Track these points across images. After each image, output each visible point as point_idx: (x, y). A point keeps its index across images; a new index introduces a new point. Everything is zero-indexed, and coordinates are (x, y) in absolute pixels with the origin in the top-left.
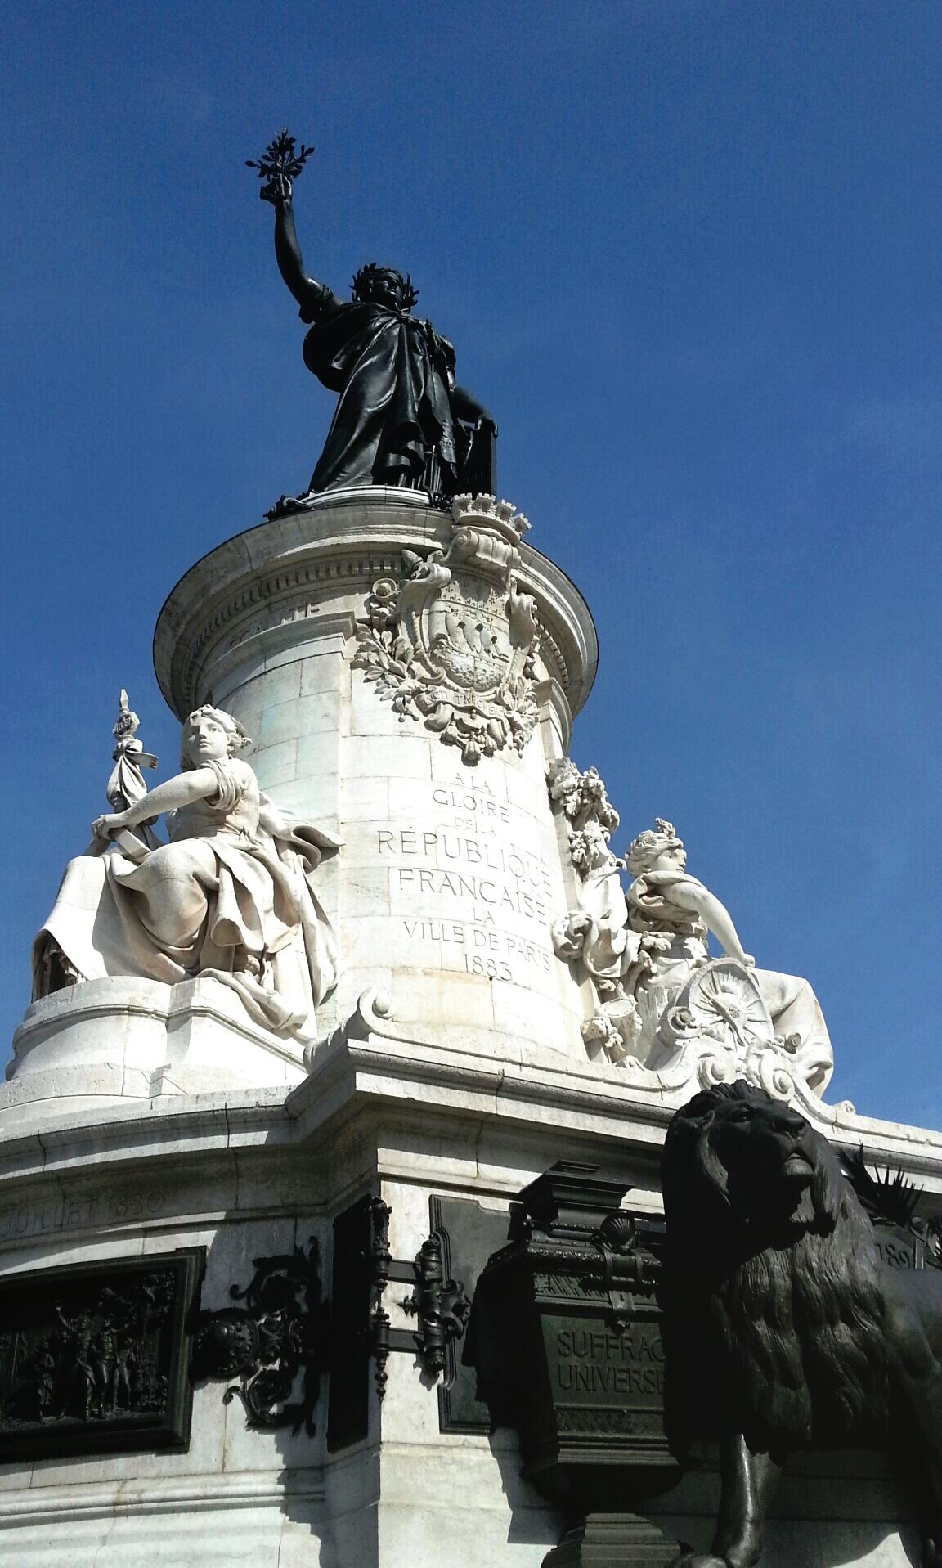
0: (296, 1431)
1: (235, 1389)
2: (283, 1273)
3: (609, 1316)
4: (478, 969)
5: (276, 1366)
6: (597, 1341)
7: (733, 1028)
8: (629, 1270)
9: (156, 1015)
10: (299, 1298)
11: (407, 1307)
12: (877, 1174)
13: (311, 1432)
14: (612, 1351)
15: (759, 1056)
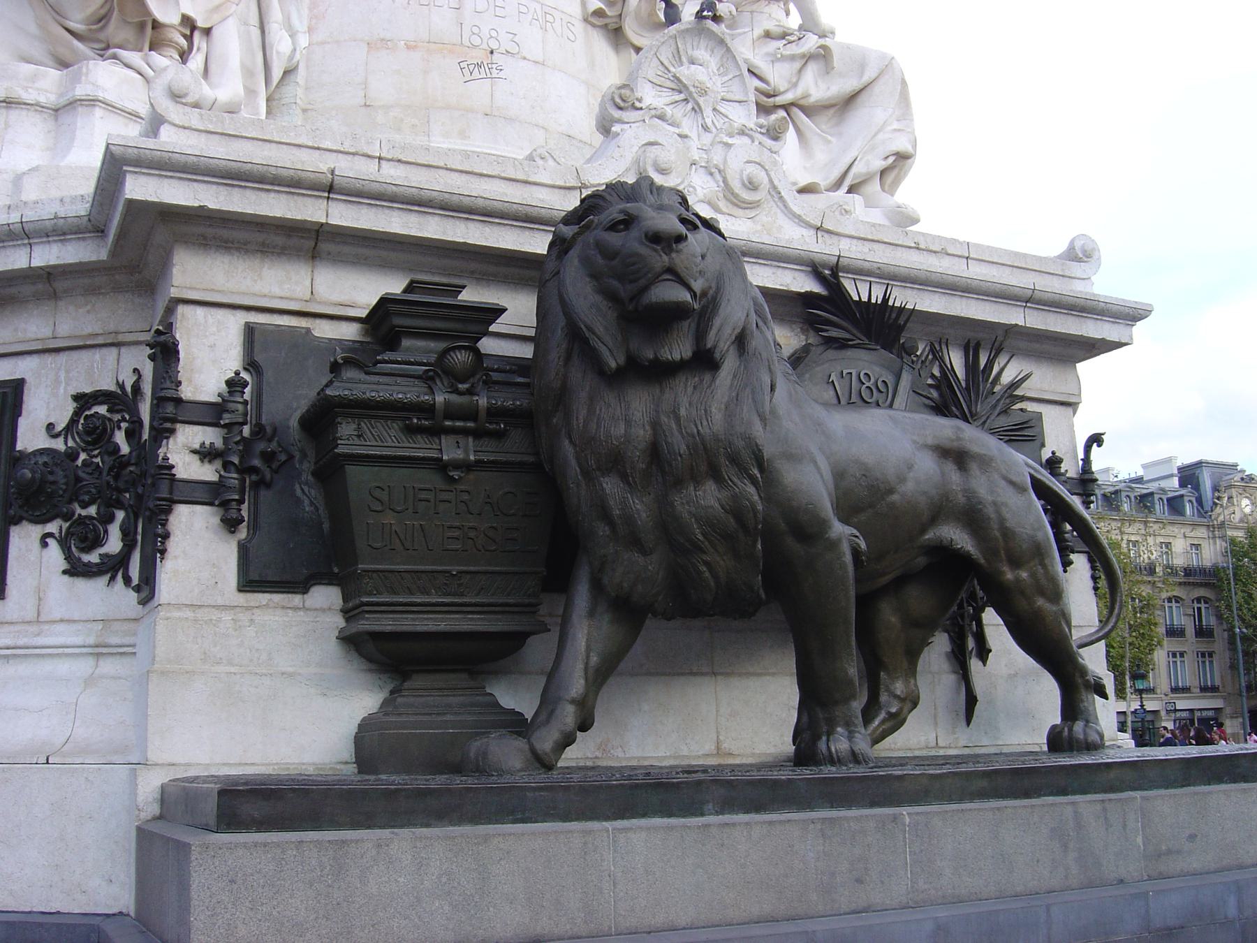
0: (113, 578)
1: (50, 535)
2: (102, 410)
3: (441, 467)
4: (477, 41)
5: (92, 511)
6: (423, 495)
7: (697, 110)
8: (471, 414)
9: (38, 107)
10: (120, 438)
11: (206, 454)
12: (857, 290)
13: (127, 580)
14: (442, 507)
15: (728, 146)
